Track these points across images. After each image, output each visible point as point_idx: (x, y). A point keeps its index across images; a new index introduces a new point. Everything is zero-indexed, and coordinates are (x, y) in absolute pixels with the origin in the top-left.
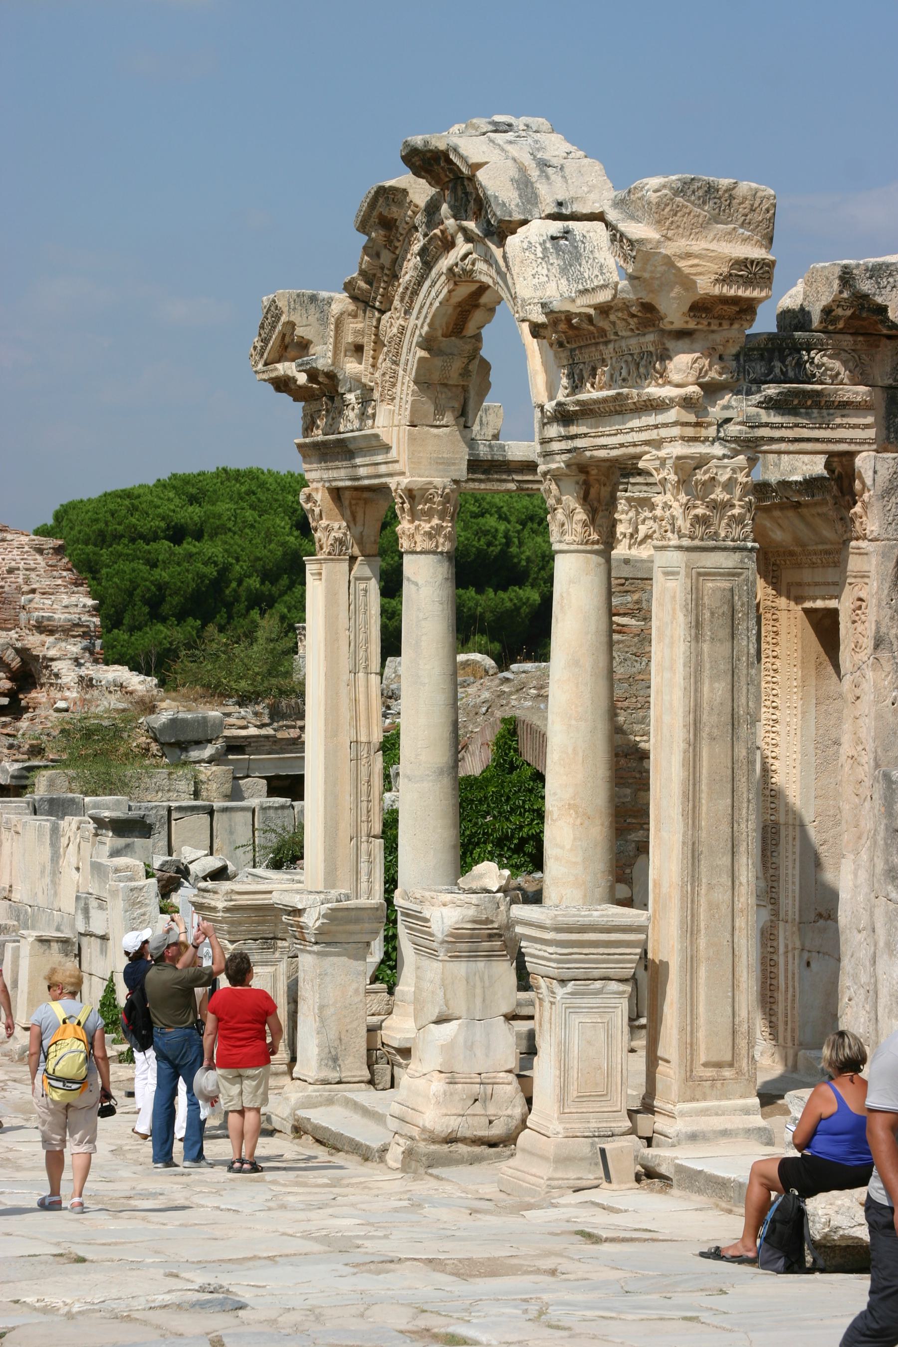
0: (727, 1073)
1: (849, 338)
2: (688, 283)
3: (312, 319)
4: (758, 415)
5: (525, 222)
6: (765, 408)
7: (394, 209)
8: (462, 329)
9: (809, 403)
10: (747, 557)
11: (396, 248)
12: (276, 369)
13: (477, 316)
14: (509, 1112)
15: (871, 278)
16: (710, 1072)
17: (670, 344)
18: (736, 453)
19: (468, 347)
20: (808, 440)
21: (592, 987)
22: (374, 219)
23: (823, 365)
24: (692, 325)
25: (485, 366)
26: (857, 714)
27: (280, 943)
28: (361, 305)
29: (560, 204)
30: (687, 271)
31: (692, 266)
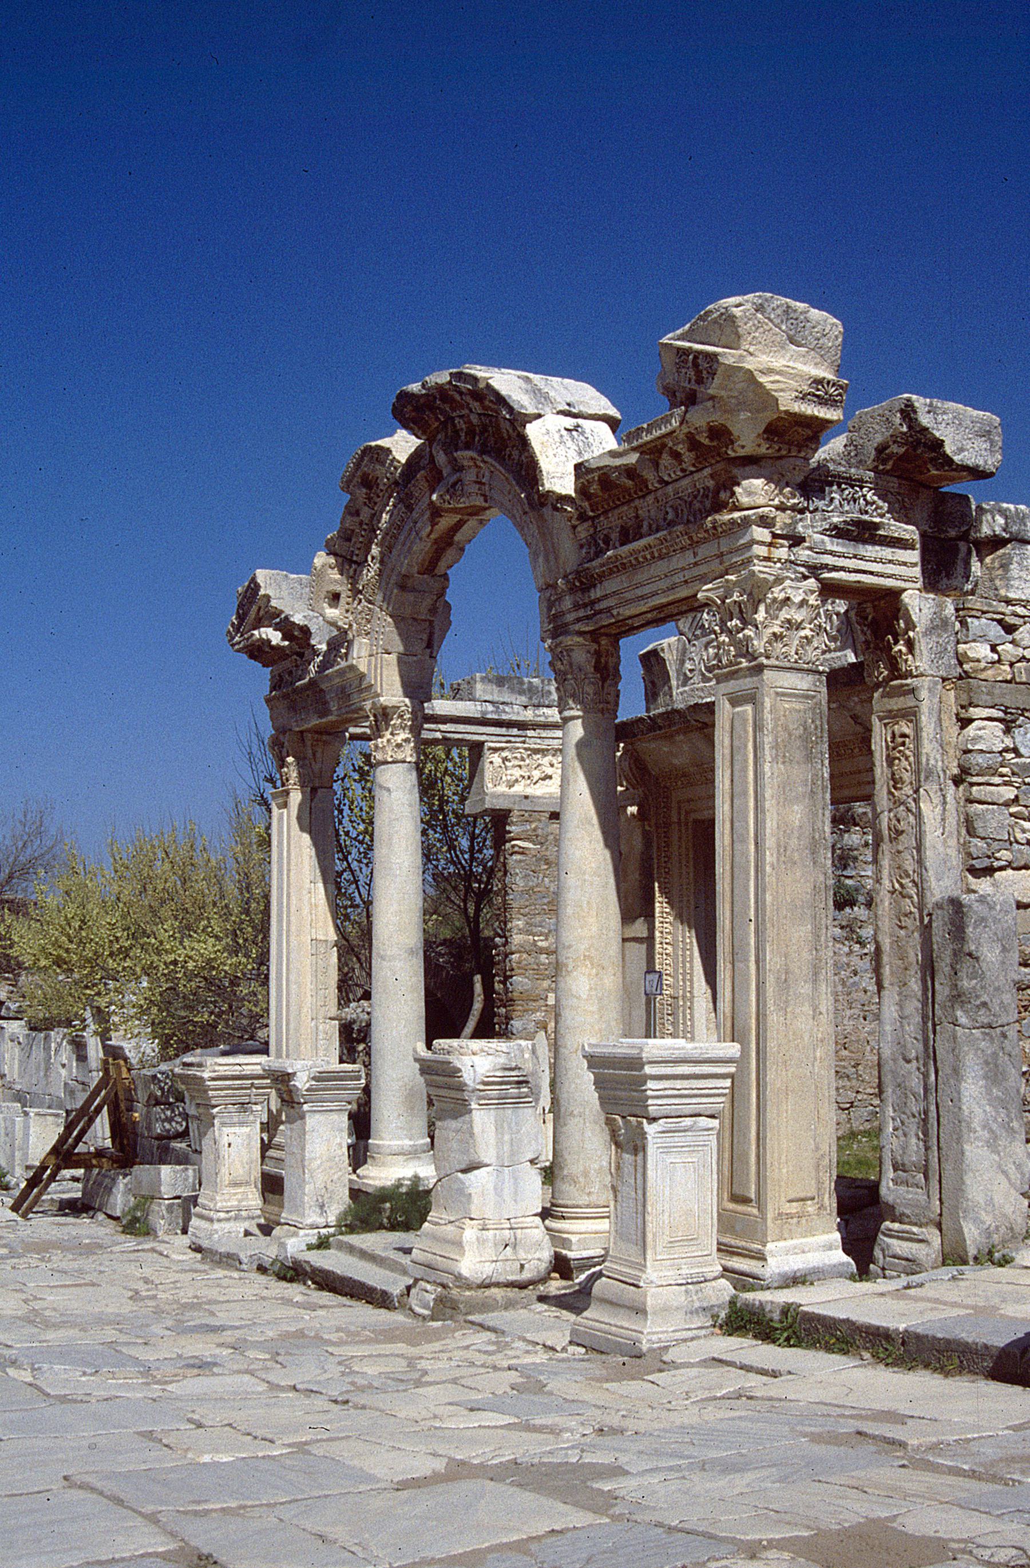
0: (811, 1207)
1: (895, 480)
2: (768, 399)
3: (285, 594)
4: (823, 542)
5: (539, 416)
6: (829, 536)
7: (378, 467)
8: (435, 567)
9: (867, 536)
10: (819, 680)
11: (375, 503)
12: (253, 635)
13: (450, 554)
14: (537, 1255)
15: (929, 412)
16: (794, 1208)
17: (736, 471)
18: (805, 578)
19: (437, 586)
20: (864, 572)
21: (683, 1124)
22: (357, 480)
23: (874, 503)
24: (763, 450)
25: (448, 606)
26: (900, 848)
27: (255, 1108)
28: (340, 560)
29: (569, 405)
30: (769, 386)
31: (772, 382)
